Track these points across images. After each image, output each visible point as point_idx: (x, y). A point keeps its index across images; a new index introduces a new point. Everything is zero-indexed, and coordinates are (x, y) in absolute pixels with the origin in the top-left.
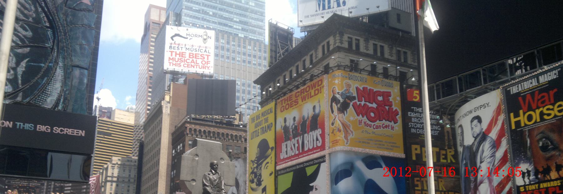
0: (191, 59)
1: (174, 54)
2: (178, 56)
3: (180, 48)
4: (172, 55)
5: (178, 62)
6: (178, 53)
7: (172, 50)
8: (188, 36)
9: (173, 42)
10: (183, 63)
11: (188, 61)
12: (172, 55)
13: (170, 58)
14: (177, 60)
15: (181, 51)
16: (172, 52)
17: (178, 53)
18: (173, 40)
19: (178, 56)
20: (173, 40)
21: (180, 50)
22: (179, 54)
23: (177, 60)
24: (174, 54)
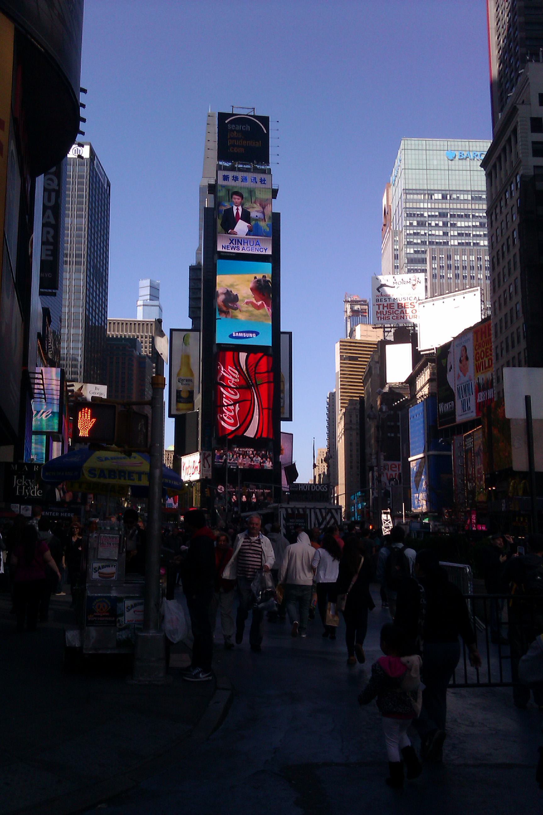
0: (400, 310)
1: (381, 307)
2: (386, 308)
3: (388, 300)
4: (379, 309)
5: (387, 315)
6: (385, 305)
7: (380, 303)
8: (395, 285)
9: (379, 294)
10: (392, 315)
11: (397, 312)
12: (379, 309)
13: (377, 312)
14: (385, 313)
15: (389, 303)
16: (379, 305)
17: (385, 305)
18: (379, 292)
19: (386, 308)
20: (379, 292)
21: (388, 302)
22: (387, 306)
23: (385, 313)
24: (381, 307)
